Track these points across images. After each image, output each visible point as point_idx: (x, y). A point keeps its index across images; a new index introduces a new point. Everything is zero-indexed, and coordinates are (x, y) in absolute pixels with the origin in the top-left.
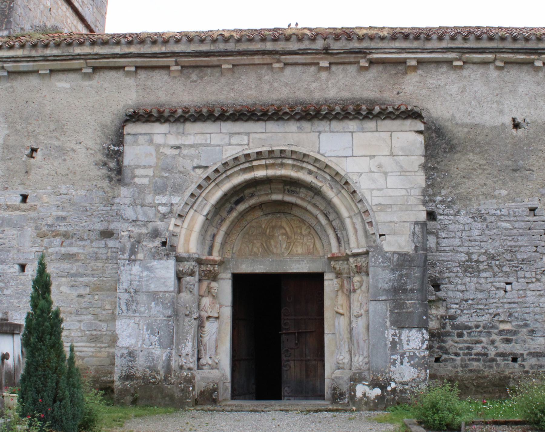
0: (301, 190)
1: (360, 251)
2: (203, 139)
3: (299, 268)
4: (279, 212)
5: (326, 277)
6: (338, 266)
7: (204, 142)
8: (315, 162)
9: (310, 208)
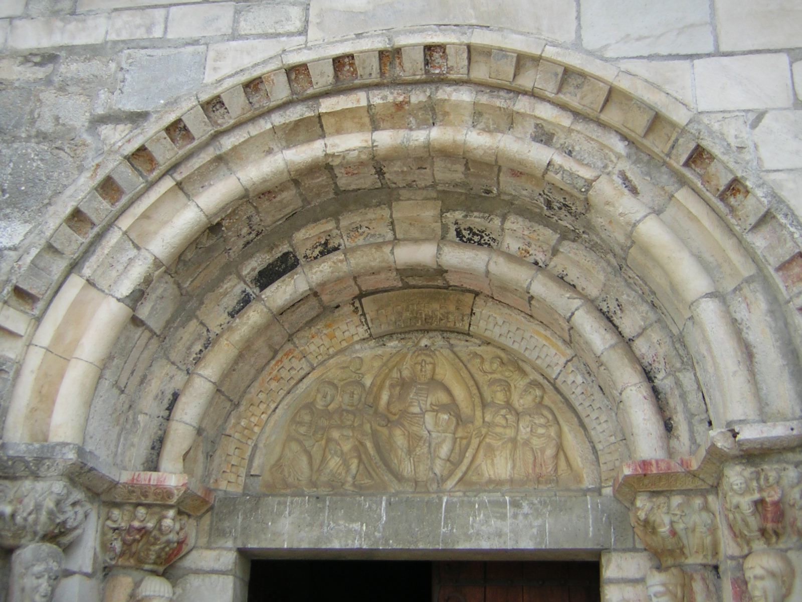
0: (508, 225)
1: (778, 431)
2: (138, 27)
3: (500, 535)
5: (610, 570)
6: (666, 519)
7: (140, 34)
8: (559, 90)
9: (541, 287)
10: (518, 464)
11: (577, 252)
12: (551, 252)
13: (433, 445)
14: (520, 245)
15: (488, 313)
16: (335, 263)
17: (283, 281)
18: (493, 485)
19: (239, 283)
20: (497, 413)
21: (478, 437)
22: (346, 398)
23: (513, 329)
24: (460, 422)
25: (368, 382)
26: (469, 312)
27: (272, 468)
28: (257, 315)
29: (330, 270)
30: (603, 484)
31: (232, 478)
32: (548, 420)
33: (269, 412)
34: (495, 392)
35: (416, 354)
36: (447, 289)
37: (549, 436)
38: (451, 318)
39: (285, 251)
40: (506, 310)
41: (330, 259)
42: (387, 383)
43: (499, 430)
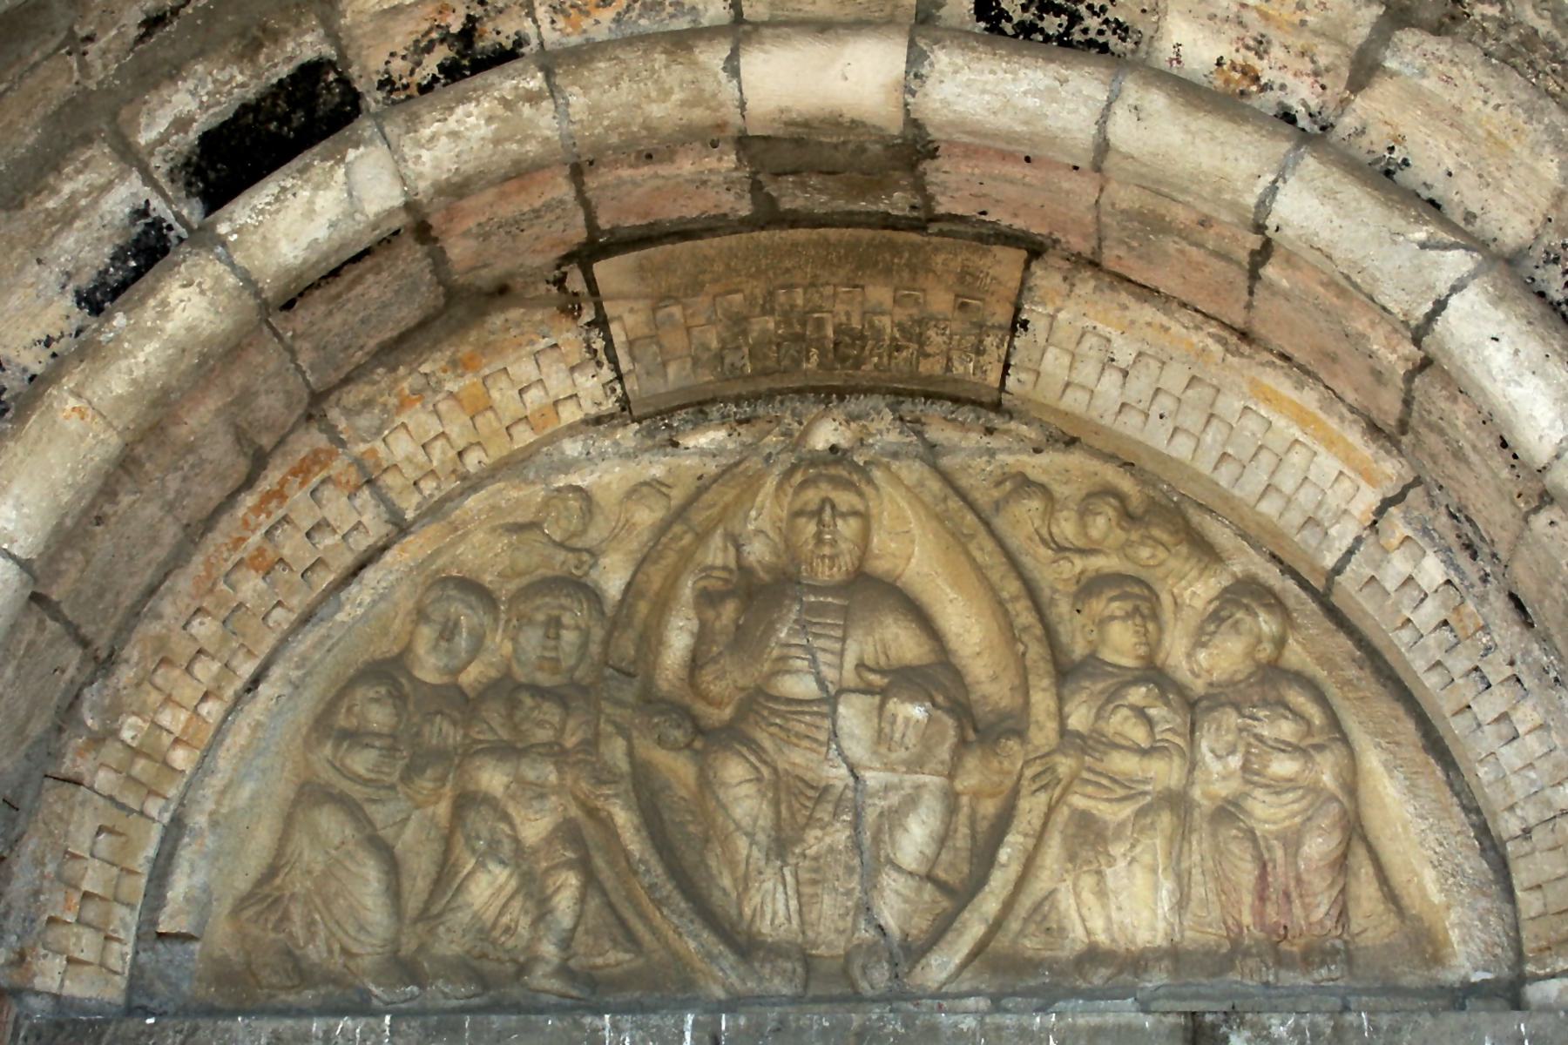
4: (830, 394)
10: (1198, 891)
11: (1454, 72)
12: (1345, 73)
13: (870, 816)
14: (1227, 51)
15: (1079, 324)
16: (505, 102)
17: (302, 171)
18: (1104, 972)
19: (122, 176)
20: (1112, 697)
21: (1043, 787)
22: (532, 639)
23: (1175, 378)
24: (971, 735)
25: (613, 579)
26: (1002, 315)
27: (236, 911)
28: (196, 299)
29: (485, 131)
30: (1530, 968)
31: (86, 945)
32: (1309, 723)
33: (229, 693)
34: (1103, 622)
35: (798, 478)
36: (918, 226)
37: (1315, 789)
38: (936, 338)
39: (309, 55)
40: (1147, 313)
41: (487, 88)
42: (687, 589)
43: (1124, 763)
